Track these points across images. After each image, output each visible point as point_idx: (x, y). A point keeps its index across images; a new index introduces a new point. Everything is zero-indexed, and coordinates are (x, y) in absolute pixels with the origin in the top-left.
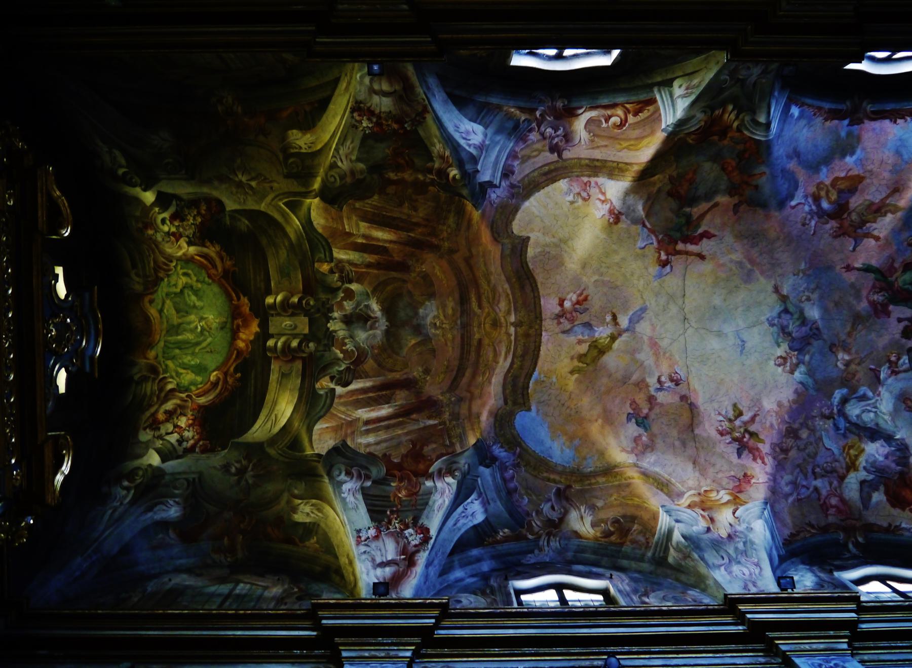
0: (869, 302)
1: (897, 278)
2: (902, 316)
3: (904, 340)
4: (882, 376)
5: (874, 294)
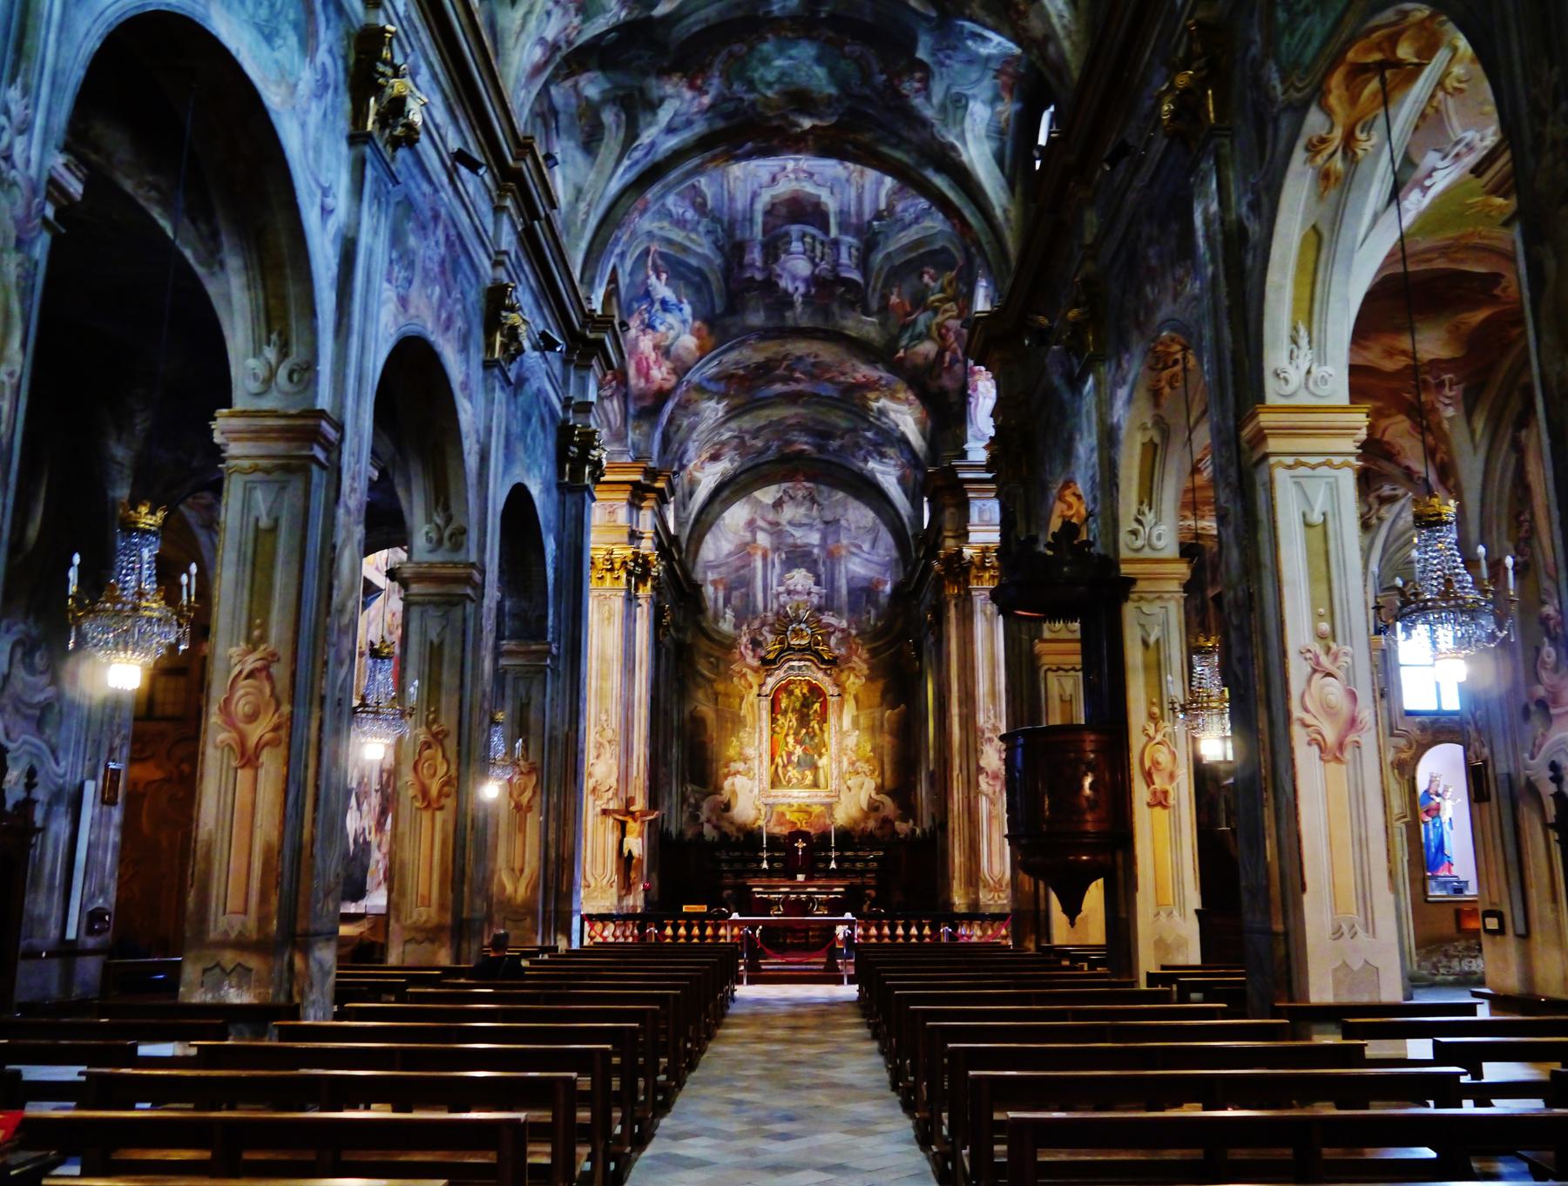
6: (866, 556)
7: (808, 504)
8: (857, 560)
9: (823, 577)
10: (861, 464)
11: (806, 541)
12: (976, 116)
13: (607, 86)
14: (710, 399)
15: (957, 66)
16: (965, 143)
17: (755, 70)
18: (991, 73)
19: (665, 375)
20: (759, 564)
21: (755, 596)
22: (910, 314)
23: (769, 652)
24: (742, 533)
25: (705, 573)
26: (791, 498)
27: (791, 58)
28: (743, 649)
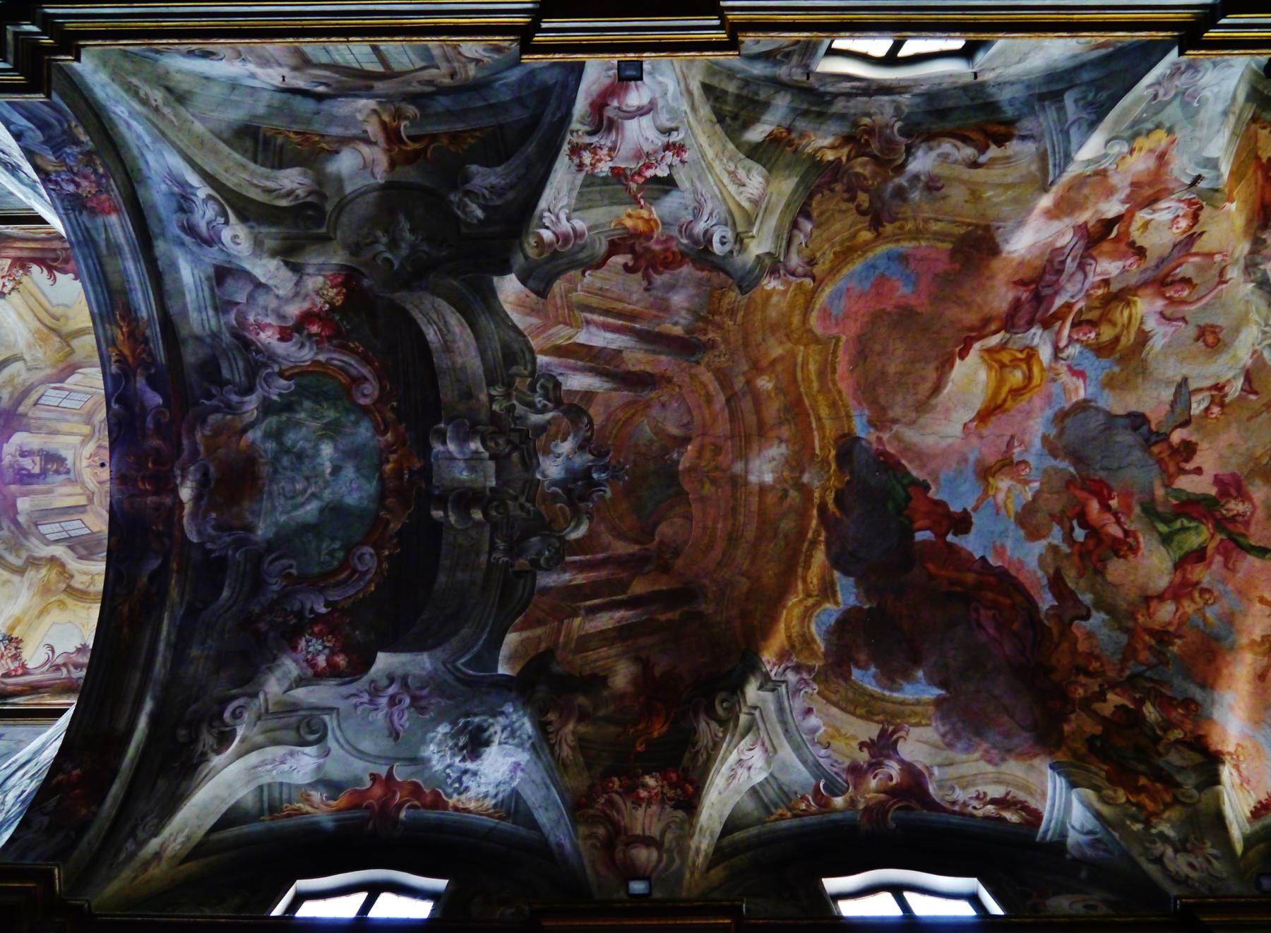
0: (1250, 499)
1: (1212, 536)
2: (1195, 477)
3: (1194, 439)
4: (1239, 383)
5: (1243, 515)
12: (291, 762)
13: (349, 189)
15: (380, 716)
16: (240, 755)
17: (313, 415)
18: (383, 771)
27: (336, 470)
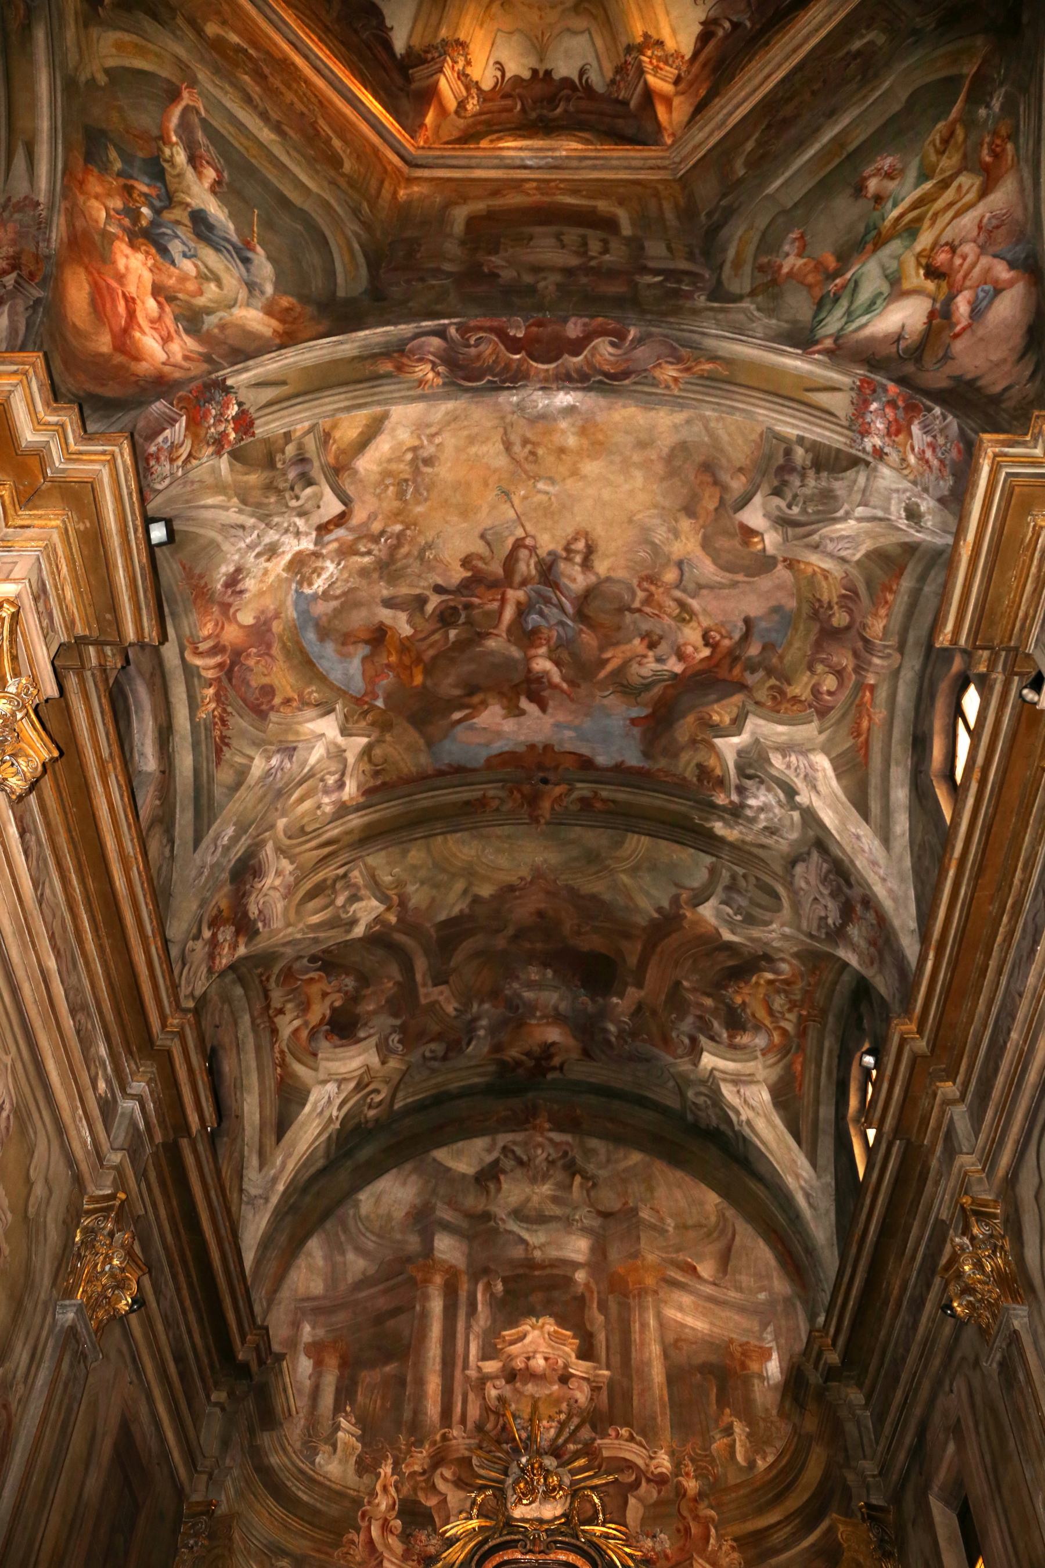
6: (708, 1290)
7: (559, 1175)
8: (687, 1299)
9: (601, 1337)
10: (684, 1066)
11: (554, 1253)
14: (326, 709)
19: (178, 358)
20: (436, 1306)
21: (420, 1382)
22: (838, 273)
23: (451, 1542)
24: (398, 1236)
25: (296, 1325)
26: (521, 1163)
28: (375, 1533)
